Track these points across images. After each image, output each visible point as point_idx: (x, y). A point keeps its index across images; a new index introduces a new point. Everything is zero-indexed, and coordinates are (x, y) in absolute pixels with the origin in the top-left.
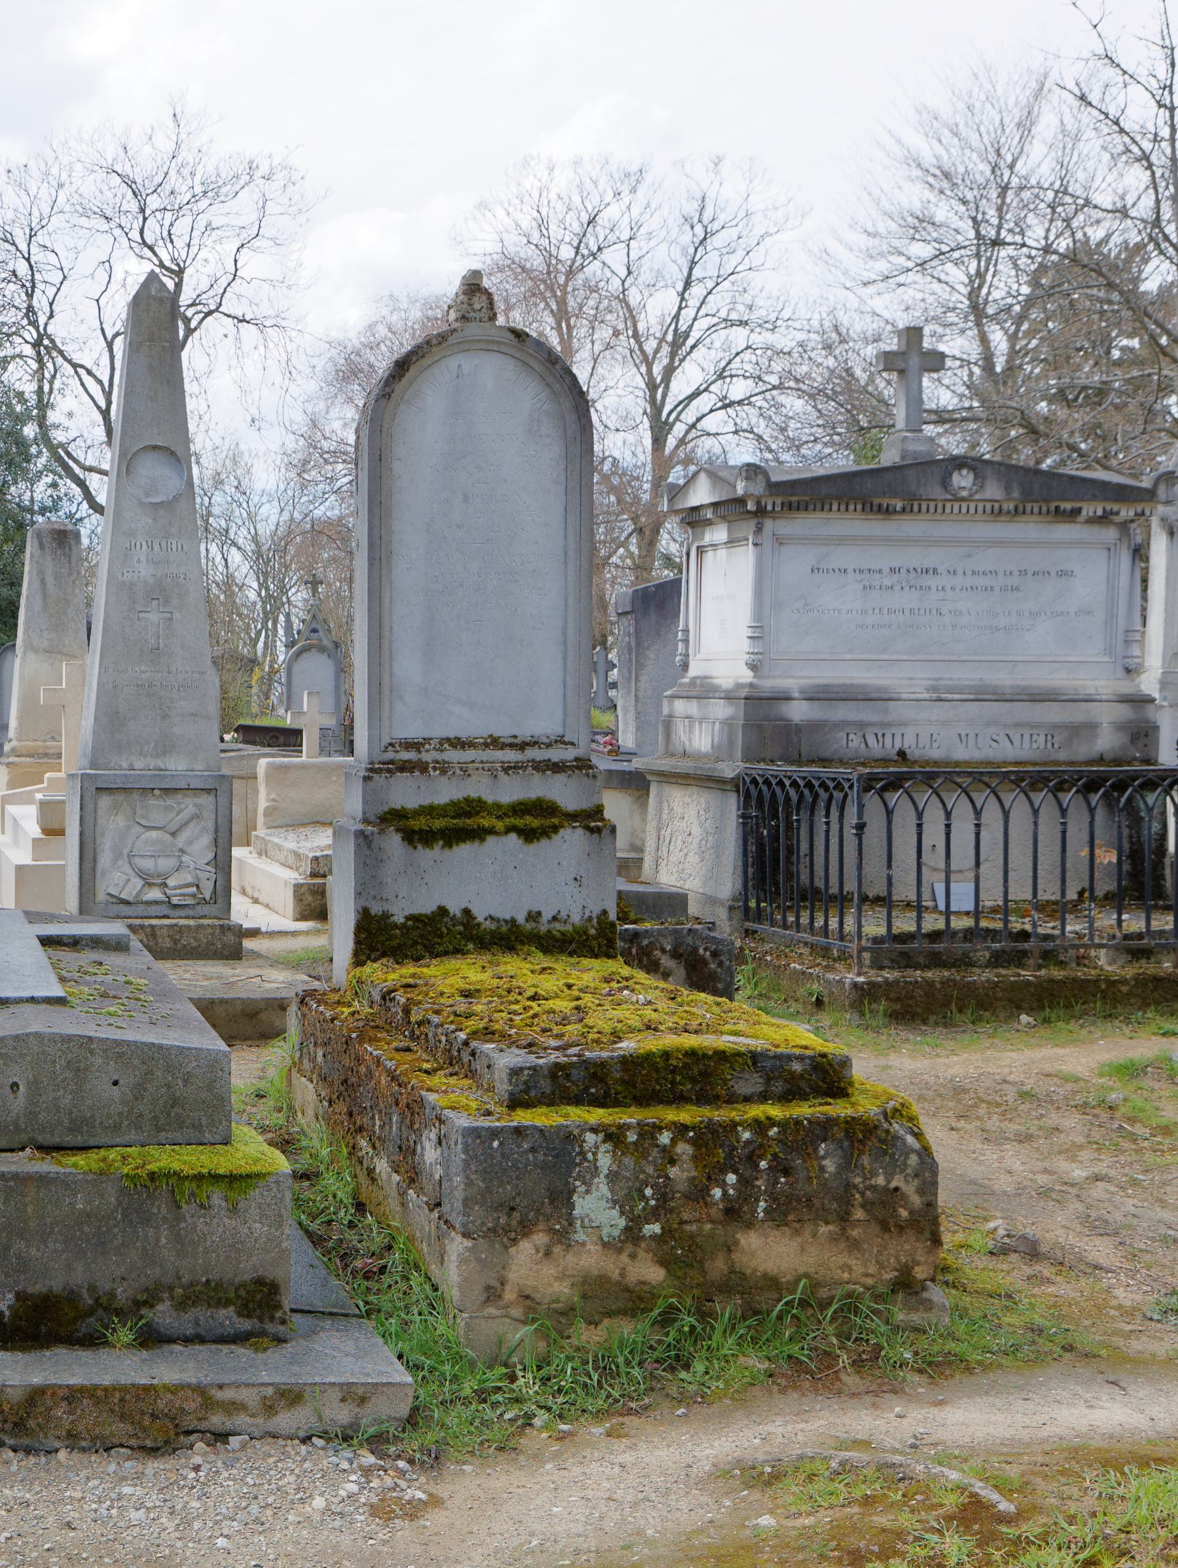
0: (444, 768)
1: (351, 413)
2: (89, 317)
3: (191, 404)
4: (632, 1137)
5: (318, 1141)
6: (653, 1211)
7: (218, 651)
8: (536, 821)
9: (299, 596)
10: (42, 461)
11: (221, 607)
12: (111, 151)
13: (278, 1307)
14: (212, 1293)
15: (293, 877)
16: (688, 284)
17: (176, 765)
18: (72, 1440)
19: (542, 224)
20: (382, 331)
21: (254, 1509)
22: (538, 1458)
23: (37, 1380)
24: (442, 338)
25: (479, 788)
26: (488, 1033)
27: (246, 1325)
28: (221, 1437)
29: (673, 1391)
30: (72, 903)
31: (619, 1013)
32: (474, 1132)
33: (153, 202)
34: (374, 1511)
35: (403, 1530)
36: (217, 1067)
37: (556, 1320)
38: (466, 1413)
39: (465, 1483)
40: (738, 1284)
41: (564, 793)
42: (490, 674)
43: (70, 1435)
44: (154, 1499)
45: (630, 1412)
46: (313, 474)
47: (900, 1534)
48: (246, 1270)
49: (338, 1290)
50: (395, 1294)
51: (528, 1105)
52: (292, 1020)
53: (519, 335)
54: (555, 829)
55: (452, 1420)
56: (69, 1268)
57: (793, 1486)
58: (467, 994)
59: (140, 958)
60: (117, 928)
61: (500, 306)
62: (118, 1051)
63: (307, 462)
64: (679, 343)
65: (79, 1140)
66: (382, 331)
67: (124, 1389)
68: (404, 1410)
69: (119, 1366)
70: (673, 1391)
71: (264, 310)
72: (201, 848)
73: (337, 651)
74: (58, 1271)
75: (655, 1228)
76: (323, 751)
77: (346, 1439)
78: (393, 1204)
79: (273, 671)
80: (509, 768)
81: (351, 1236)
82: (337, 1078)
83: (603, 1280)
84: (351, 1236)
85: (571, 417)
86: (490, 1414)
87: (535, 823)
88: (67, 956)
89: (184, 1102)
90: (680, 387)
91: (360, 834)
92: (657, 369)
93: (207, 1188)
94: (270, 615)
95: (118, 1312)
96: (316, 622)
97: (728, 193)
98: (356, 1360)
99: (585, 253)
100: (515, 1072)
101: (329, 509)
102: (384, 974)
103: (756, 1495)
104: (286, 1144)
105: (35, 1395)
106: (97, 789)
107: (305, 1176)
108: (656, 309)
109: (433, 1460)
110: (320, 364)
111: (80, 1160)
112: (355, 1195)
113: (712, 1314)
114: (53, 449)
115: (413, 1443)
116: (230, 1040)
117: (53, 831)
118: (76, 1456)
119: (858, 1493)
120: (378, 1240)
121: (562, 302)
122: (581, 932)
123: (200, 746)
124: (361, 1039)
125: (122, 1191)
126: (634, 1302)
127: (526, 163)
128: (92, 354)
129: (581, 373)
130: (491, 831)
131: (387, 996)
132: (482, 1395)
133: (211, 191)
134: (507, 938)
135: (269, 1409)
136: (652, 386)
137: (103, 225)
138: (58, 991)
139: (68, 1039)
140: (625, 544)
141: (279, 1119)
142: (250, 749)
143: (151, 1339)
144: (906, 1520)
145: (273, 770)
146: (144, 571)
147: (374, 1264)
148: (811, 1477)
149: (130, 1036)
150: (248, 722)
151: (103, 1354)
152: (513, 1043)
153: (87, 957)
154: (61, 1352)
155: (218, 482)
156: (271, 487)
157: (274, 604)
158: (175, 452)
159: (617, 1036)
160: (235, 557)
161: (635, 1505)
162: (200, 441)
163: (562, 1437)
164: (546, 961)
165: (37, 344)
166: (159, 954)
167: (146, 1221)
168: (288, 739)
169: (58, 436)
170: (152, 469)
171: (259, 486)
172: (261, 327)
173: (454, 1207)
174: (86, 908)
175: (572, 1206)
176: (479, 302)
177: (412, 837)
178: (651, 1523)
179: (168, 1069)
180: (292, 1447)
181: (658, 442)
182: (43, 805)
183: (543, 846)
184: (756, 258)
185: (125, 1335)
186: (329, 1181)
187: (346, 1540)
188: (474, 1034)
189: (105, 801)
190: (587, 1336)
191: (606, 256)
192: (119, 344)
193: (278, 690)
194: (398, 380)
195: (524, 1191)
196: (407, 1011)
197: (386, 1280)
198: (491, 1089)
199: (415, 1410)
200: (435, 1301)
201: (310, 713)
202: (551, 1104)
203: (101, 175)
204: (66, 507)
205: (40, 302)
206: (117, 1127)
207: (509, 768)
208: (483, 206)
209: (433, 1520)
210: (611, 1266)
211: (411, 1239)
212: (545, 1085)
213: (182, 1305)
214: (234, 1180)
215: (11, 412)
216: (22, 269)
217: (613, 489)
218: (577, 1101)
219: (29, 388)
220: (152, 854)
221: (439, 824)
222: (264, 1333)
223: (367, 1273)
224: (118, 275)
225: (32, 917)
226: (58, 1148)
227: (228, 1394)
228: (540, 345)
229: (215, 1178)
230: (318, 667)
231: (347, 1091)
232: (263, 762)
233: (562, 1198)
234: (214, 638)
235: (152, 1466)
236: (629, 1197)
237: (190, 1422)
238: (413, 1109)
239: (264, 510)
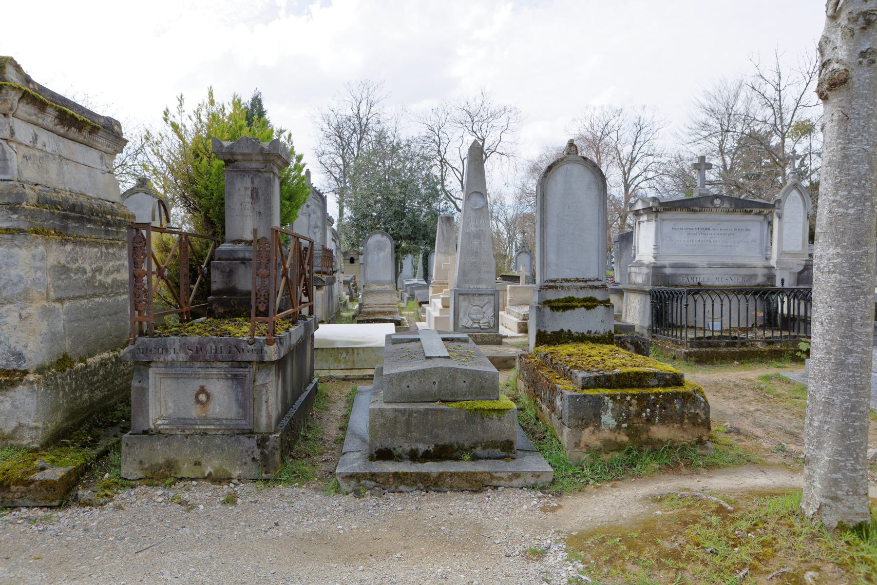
0: (562, 288)
1: (535, 182)
2: (456, 153)
3: (487, 179)
4: (619, 398)
5: (525, 399)
6: (625, 420)
7: (495, 253)
8: (590, 304)
9: (519, 236)
10: (442, 196)
11: (496, 240)
12: (463, 104)
13: (513, 448)
14: (493, 445)
15: (517, 320)
16: (635, 143)
17: (483, 287)
18: (452, 488)
19: (592, 126)
20: (544, 157)
21: (506, 509)
22: (590, 494)
23: (441, 470)
24: (562, 159)
25: (573, 294)
26: (576, 367)
27: (503, 454)
28: (496, 487)
29: (631, 474)
30: (451, 328)
31: (614, 361)
32: (572, 396)
33: (476, 119)
34: (542, 509)
35: (550, 515)
36: (495, 377)
37: (596, 453)
38: (569, 480)
39: (569, 501)
40: (650, 442)
41: (598, 295)
42: (576, 259)
43: (451, 487)
44: (476, 506)
45: (618, 480)
46: (523, 200)
47: (698, 516)
48: (503, 438)
49: (531, 444)
50: (548, 445)
51: (587, 388)
52: (517, 363)
53: (585, 158)
54: (596, 306)
55: (565, 482)
56: (451, 437)
57: (666, 502)
58: (569, 355)
59: (472, 344)
60: (465, 336)
61: (579, 150)
62: (465, 372)
63: (522, 196)
64: (632, 161)
65: (454, 399)
66: (544, 157)
67: (467, 473)
68: (551, 480)
69: (465, 466)
70: (631, 474)
71: (509, 151)
72: (490, 312)
73: (531, 253)
74: (447, 438)
75: (626, 425)
76: (526, 282)
77: (533, 488)
78: (547, 418)
79: (512, 259)
80: (582, 288)
81: (535, 427)
82: (531, 380)
83: (610, 440)
84: (535, 427)
85: (600, 183)
86: (576, 481)
87: (590, 304)
88: (450, 344)
89: (485, 387)
90: (633, 174)
91: (537, 307)
92: (626, 169)
93: (492, 413)
94: (511, 242)
95: (465, 450)
96: (524, 244)
97: (647, 116)
98: (536, 464)
99: (605, 134)
100: (584, 378)
101: (528, 210)
102: (544, 349)
103: (656, 505)
104: (515, 400)
105: (441, 475)
106: (459, 294)
107: (521, 410)
108: (626, 151)
109: (559, 494)
110: (525, 167)
111: (454, 405)
112: (536, 415)
113: (642, 451)
114: (446, 193)
115: (553, 489)
116: (499, 369)
117: (446, 306)
118: (453, 493)
119: (686, 504)
120: (543, 429)
121: (598, 149)
122: (603, 337)
123: (489, 281)
124: (538, 369)
125: (467, 414)
126: (619, 447)
127: (587, 107)
128: (457, 164)
129: (603, 170)
130: (577, 307)
131: (545, 356)
132: (574, 475)
133: (493, 116)
134: (581, 339)
135: (510, 479)
136: (625, 174)
137: (460, 126)
138: (447, 355)
139: (451, 368)
140: (616, 221)
141: (513, 392)
142: (505, 282)
143: (475, 458)
144: (700, 512)
145: (512, 289)
146: (473, 229)
147: (542, 436)
148: (672, 499)
149: (469, 368)
150: (504, 274)
151: (461, 462)
152: (583, 370)
153: (456, 344)
154: (448, 462)
155: (495, 202)
156: (511, 204)
157: (512, 239)
158: (482, 193)
159: (614, 368)
160: (500, 225)
161: (619, 508)
162: (490, 190)
163: (598, 487)
164: (593, 345)
165: (441, 161)
166: (477, 343)
167: (474, 422)
168: (516, 279)
169: (447, 189)
170: (475, 198)
171: (507, 204)
172: (508, 156)
173: (565, 419)
174: (456, 330)
175: (601, 419)
176: (573, 149)
177: (553, 308)
178: (624, 513)
179: (480, 377)
180: (517, 490)
181: (626, 190)
182: (443, 299)
183: (592, 311)
184: (656, 135)
185: (467, 457)
186: (528, 411)
187: (533, 518)
188: (571, 367)
189: (461, 298)
190: (605, 457)
191: (611, 135)
192: (465, 161)
193: (513, 264)
194: (548, 171)
195: (586, 414)
196: (551, 360)
197: (545, 440)
198: (576, 384)
199: (554, 479)
200: (560, 447)
201: (522, 271)
202: (594, 388)
203: (460, 111)
204: (450, 210)
205: (442, 149)
206: (465, 395)
207: (582, 288)
208: (574, 120)
209: (559, 512)
210: (612, 436)
211: (553, 428)
212: (593, 382)
213: (484, 448)
214: (499, 411)
215: (433, 181)
216: (437, 139)
217: (613, 205)
218: (602, 387)
219: (439, 174)
220: (475, 313)
221: (561, 304)
222: (509, 456)
223: (540, 438)
224: (465, 140)
225: (440, 332)
226: (447, 401)
227: (498, 475)
228: (591, 161)
229: (494, 410)
230: (525, 258)
231: (533, 384)
232: (509, 286)
233: (598, 416)
234: (494, 249)
235: (475, 496)
236: (618, 416)
237: (486, 483)
238: (553, 390)
239: (509, 211)
